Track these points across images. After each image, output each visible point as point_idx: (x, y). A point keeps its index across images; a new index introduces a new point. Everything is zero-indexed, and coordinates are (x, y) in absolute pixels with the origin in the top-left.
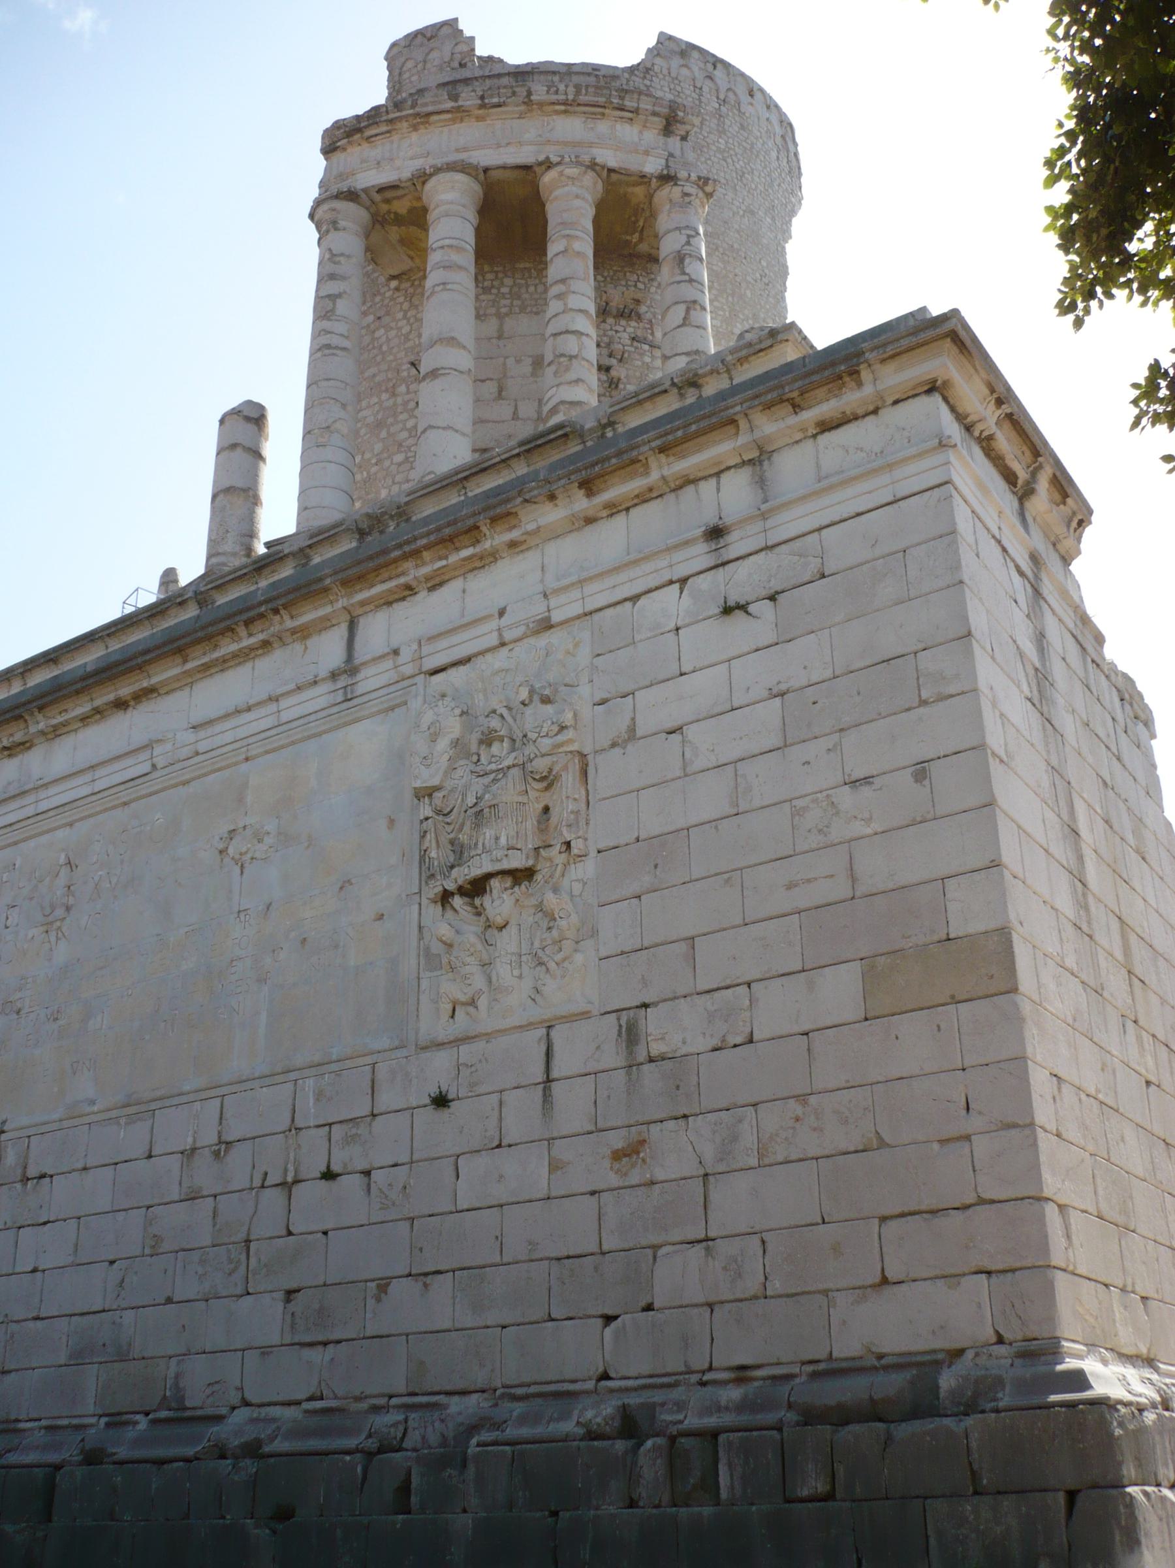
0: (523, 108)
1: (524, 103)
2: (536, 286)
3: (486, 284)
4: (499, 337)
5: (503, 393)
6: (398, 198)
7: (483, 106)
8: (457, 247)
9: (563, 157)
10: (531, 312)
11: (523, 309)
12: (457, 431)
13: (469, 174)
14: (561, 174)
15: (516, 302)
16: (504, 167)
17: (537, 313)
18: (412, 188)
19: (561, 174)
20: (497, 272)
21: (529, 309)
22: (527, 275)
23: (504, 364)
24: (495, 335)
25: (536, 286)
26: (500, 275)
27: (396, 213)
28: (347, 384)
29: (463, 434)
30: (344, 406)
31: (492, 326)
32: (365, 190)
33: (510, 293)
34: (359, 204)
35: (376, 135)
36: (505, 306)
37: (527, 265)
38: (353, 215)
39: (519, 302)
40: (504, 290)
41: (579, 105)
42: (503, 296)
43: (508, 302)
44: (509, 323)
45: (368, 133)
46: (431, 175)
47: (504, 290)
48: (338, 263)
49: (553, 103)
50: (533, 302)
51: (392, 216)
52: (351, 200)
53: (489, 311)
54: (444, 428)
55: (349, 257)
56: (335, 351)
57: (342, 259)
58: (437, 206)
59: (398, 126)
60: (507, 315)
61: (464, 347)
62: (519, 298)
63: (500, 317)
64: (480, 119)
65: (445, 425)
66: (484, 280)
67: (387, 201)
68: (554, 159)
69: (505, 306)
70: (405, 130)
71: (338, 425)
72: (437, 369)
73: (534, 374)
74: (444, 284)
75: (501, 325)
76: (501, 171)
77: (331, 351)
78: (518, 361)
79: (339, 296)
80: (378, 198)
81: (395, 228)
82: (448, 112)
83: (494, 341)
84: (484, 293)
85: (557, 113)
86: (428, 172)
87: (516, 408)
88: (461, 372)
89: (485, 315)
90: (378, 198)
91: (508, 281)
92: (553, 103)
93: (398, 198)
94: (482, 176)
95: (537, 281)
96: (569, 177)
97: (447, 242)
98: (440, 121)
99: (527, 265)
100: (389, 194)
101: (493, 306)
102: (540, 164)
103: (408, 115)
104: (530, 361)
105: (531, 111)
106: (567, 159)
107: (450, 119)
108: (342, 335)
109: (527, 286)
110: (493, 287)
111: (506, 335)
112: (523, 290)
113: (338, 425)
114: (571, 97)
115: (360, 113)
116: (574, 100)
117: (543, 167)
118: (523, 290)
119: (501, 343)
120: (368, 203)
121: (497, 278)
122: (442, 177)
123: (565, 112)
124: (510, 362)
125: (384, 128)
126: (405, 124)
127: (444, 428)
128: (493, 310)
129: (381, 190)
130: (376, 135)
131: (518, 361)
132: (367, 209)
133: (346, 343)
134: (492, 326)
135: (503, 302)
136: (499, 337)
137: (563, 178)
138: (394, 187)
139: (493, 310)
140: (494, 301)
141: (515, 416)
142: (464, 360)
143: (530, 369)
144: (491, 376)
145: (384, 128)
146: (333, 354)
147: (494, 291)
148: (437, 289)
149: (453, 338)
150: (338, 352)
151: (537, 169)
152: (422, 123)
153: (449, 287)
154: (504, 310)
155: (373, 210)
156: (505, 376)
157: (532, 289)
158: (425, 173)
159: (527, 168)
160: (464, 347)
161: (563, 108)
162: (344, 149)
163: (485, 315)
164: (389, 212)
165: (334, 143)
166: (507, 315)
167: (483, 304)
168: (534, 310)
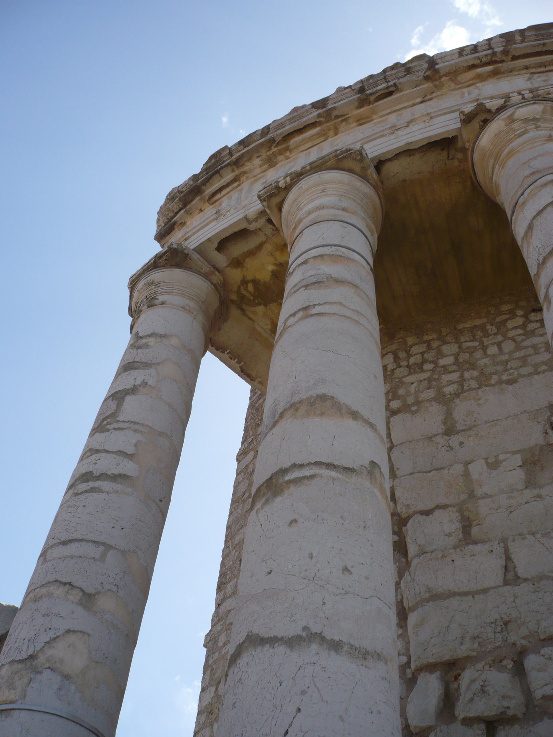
0: (427, 85)
1: (427, 78)
2: (499, 344)
3: (412, 360)
4: (450, 431)
5: (475, 531)
6: (252, 253)
7: (363, 101)
8: (330, 256)
9: (507, 97)
10: (500, 382)
11: (484, 380)
12: (335, 646)
13: (350, 171)
14: (511, 120)
15: (467, 375)
16: (407, 152)
17: (511, 382)
18: (269, 229)
19: (511, 120)
20: (428, 342)
21: (494, 379)
22: (479, 334)
23: (466, 474)
24: (441, 428)
25: (499, 344)
26: (435, 344)
27: (255, 282)
28: (108, 547)
29: (363, 655)
30: (88, 599)
31: (431, 419)
32: (199, 250)
33: (456, 362)
34: (190, 269)
35: (220, 190)
36: (450, 383)
37: (478, 322)
38: (184, 286)
39: (475, 373)
40: (443, 362)
41: (514, 58)
42: (446, 370)
43: (454, 376)
44: (461, 410)
45: (209, 190)
46: (288, 188)
47: (443, 362)
48: (146, 346)
49: (473, 67)
50: (500, 368)
51: (251, 287)
52: (178, 265)
53: (423, 396)
54: (293, 642)
55: (164, 336)
56: (97, 484)
57: (151, 341)
58: (300, 221)
59: (247, 166)
60: (457, 395)
61: (355, 415)
62: (473, 367)
63: (441, 398)
64: (361, 121)
65: (293, 630)
66: (409, 356)
67: (237, 263)
68: (493, 105)
69: (450, 383)
70: (258, 170)
71: (59, 651)
72: (283, 471)
73: (529, 483)
74: (306, 308)
75: (449, 413)
76: (404, 161)
77: (91, 484)
78: (494, 465)
79: (133, 391)
80: (221, 260)
81: (261, 309)
82: (313, 125)
83: (441, 440)
84: (410, 374)
85: (482, 78)
86: (282, 184)
87: (508, 558)
88: (347, 470)
89: (418, 403)
90: (221, 260)
91: (450, 349)
92: (473, 67)
93: (252, 253)
94: (372, 171)
95: (499, 338)
96: (526, 120)
97: (314, 253)
98: (303, 142)
99: (478, 322)
100: (238, 249)
101: (429, 388)
102: (467, 119)
103: (262, 145)
104: (517, 460)
105: (439, 87)
106: (516, 98)
107: (319, 135)
108: (121, 453)
109: (484, 348)
110: (424, 361)
111: (459, 427)
112: (478, 354)
113: (59, 651)
114: (499, 49)
115: (197, 171)
116: (505, 52)
117: (476, 124)
118: (478, 354)
119: (454, 440)
120: (206, 268)
121: (429, 348)
122: (304, 183)
123: (495, 74)
124: (477, 469)
125: (228, 176)
126: (257, 162)
127: (293, 642)
128: (431, 393)
129: (224, 243)
130: (220, 190)
131: (494, 465)
132: (206, 276)
133: (128, 467)
134: (431, 419)
135: (445, 378)
136: (450, 431)
137: (515, 125)
138: (240, 234)
139: (431, 393)
140: (429, 380)
141: (510, 575)
142: (359, 444)
143: (520, 474)
144: (442, 500)
145: (228, 176)
146: (93, 490)
147: (428, 366)
148: (292, 320)
149: (323, 398)
150: (106, 485)
151: (466, 135)
152: (281, 153)
153: (313, 311)
154: (449, 390)
155: (217, 278)
156: (472, 495)
157: (493, 350)
158: (278, 188)
159: (445, 144)
160: (355, 415)
161: (489, 68)
162: (183, 224)
163: (418, 403)
164: (244, 282)
165: (170, 220)
166: (457, 395)
167: (412, 389)
168: (505, 377)
